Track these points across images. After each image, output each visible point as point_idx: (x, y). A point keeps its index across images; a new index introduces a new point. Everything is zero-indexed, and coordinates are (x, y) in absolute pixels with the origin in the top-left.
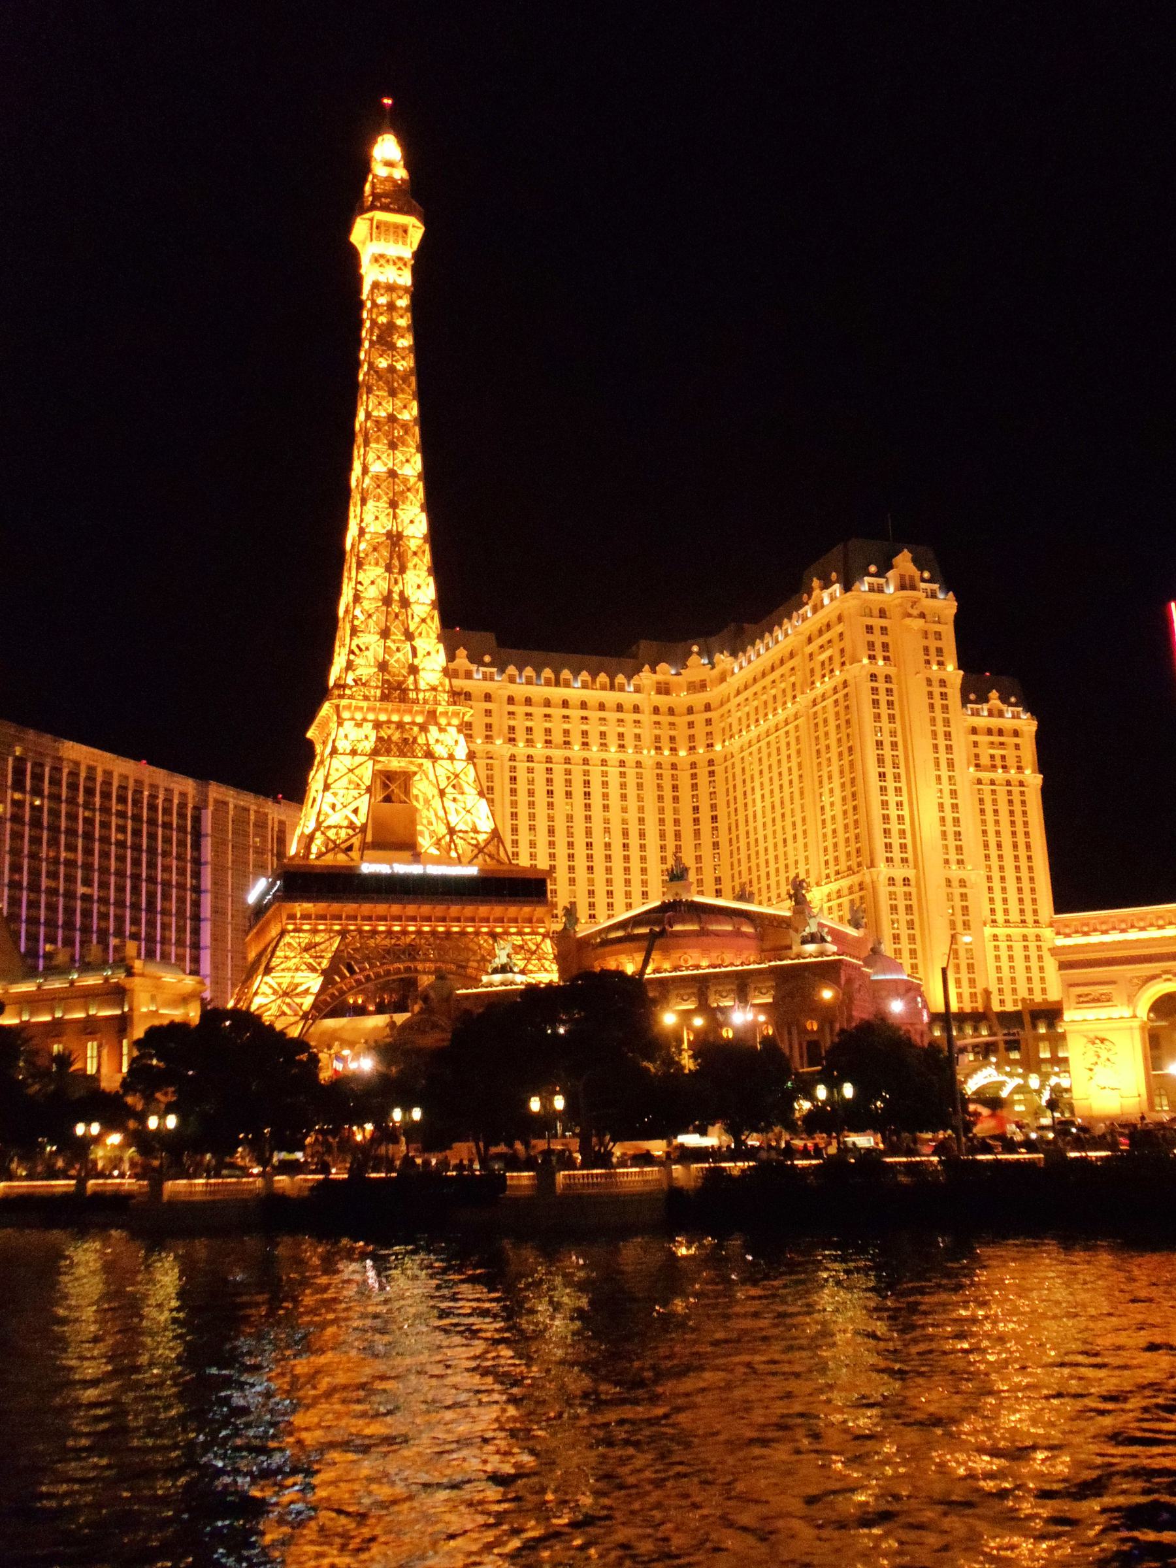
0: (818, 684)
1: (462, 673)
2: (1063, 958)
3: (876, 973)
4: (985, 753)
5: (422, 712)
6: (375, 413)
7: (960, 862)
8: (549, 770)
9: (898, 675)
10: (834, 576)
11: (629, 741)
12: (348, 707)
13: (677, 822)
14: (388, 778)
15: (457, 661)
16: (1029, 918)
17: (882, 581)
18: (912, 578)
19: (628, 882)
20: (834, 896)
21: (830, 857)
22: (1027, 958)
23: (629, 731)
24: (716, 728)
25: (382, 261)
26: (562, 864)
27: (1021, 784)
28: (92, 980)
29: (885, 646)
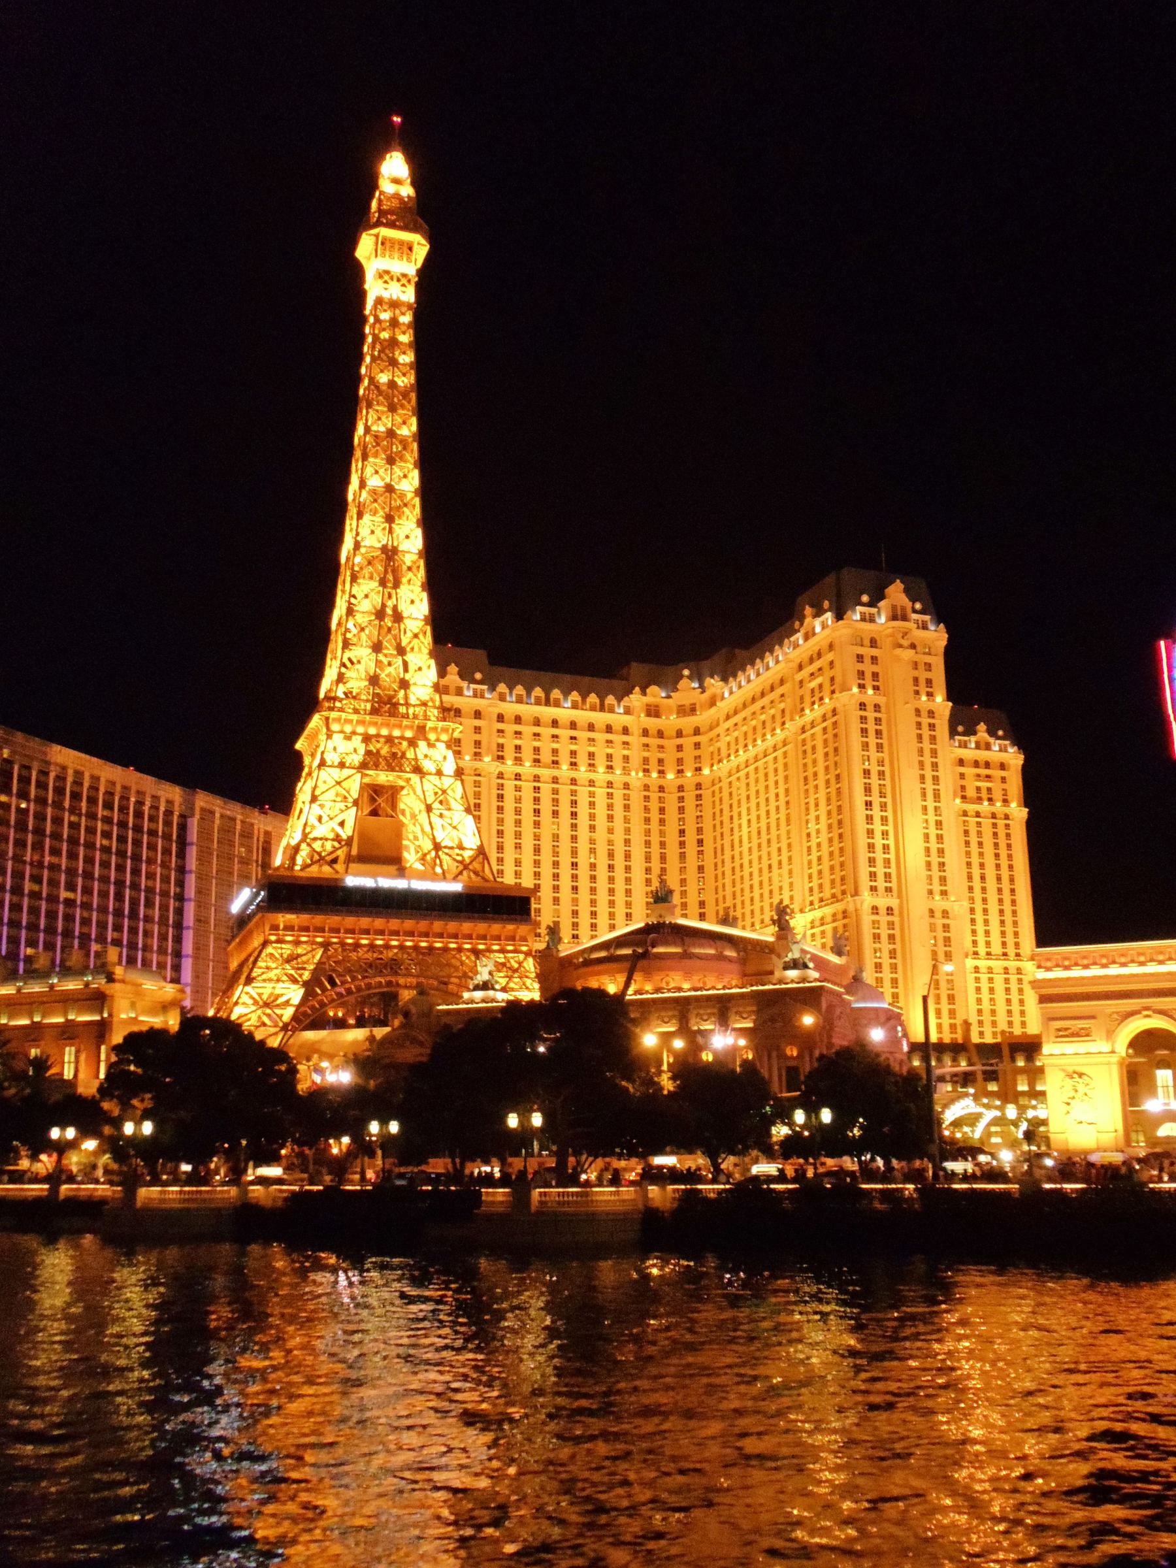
0: (807, 711)
1: (452, 689)
2: (1045, 991)
3: (856, 1001)
4: (971, 786)
5: (411, 727)
6: (374, 428)
7: (944, 893)
8: (537, 789)
9: (887, 704)
10: (826, 604)
11: (618, 763)
12: (338, 720)
13: (663, 844)
14: (375, 791)
15: (448, 677)
16: (1011, 951)
17: (874, 610)
18: (903, 609)
19: (612, 903)
20: (817, 923)
21: (815, 883)
22: (1008, 990)
23: (618, 752)
24: (705, 752)
25: (386, 278)
26: (546, 883)
27: (1007, 817)
28: (72, 985)
29: (875, 676)
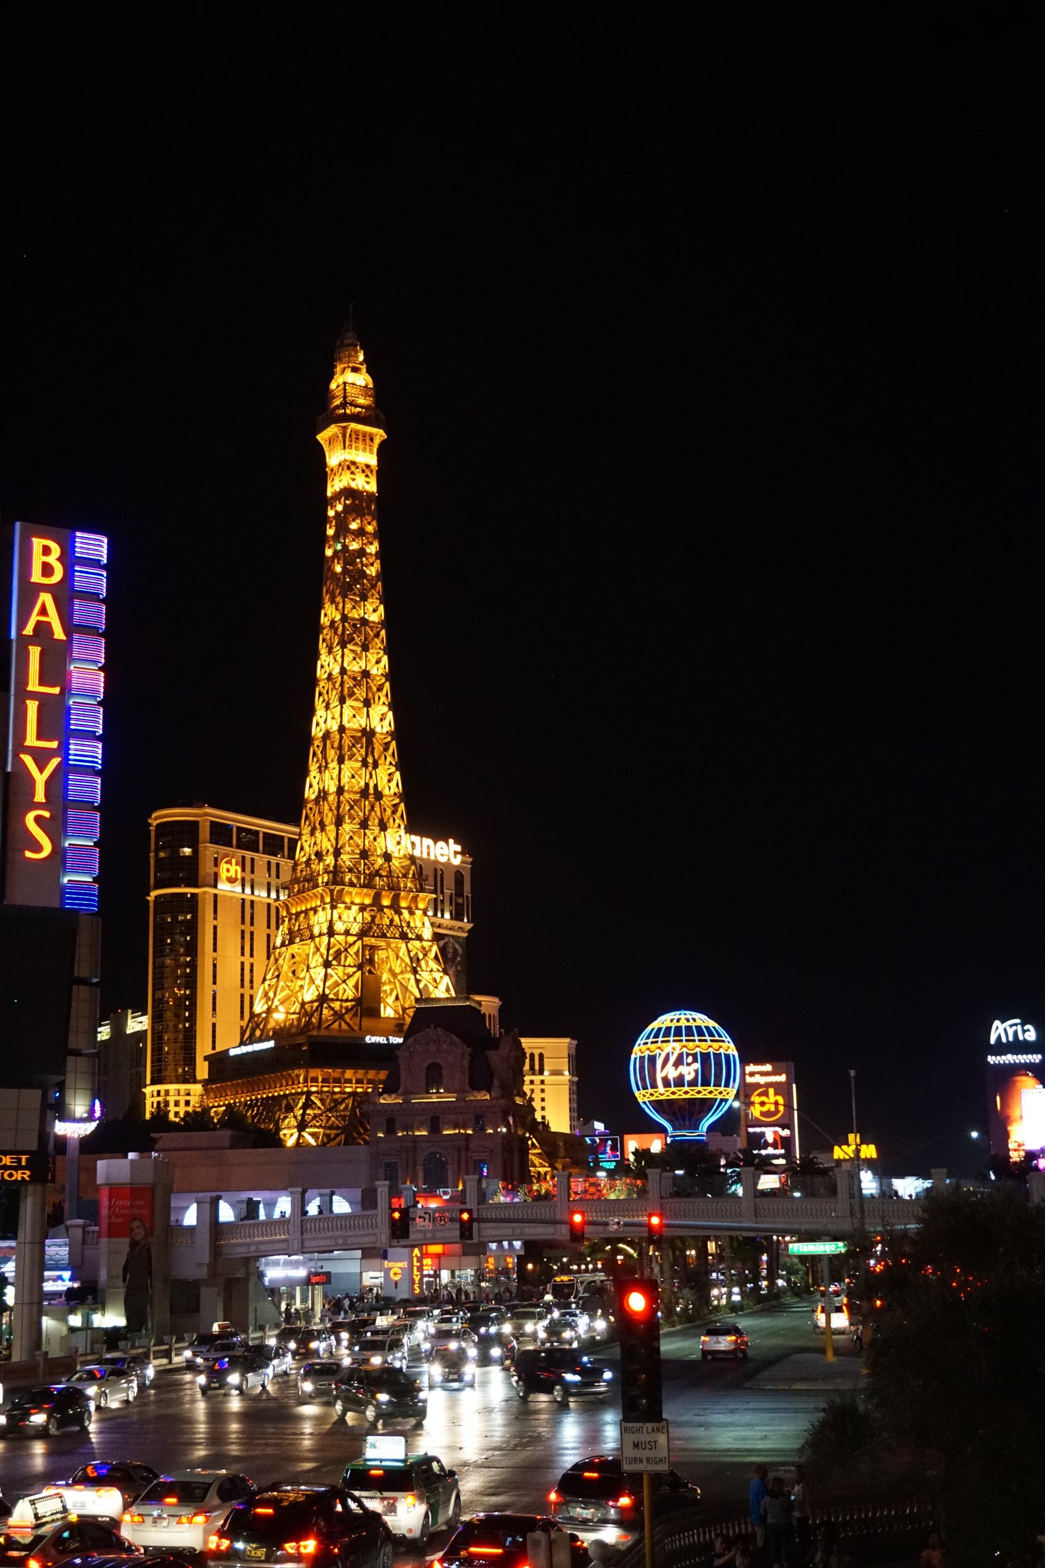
25: (353, 468)
